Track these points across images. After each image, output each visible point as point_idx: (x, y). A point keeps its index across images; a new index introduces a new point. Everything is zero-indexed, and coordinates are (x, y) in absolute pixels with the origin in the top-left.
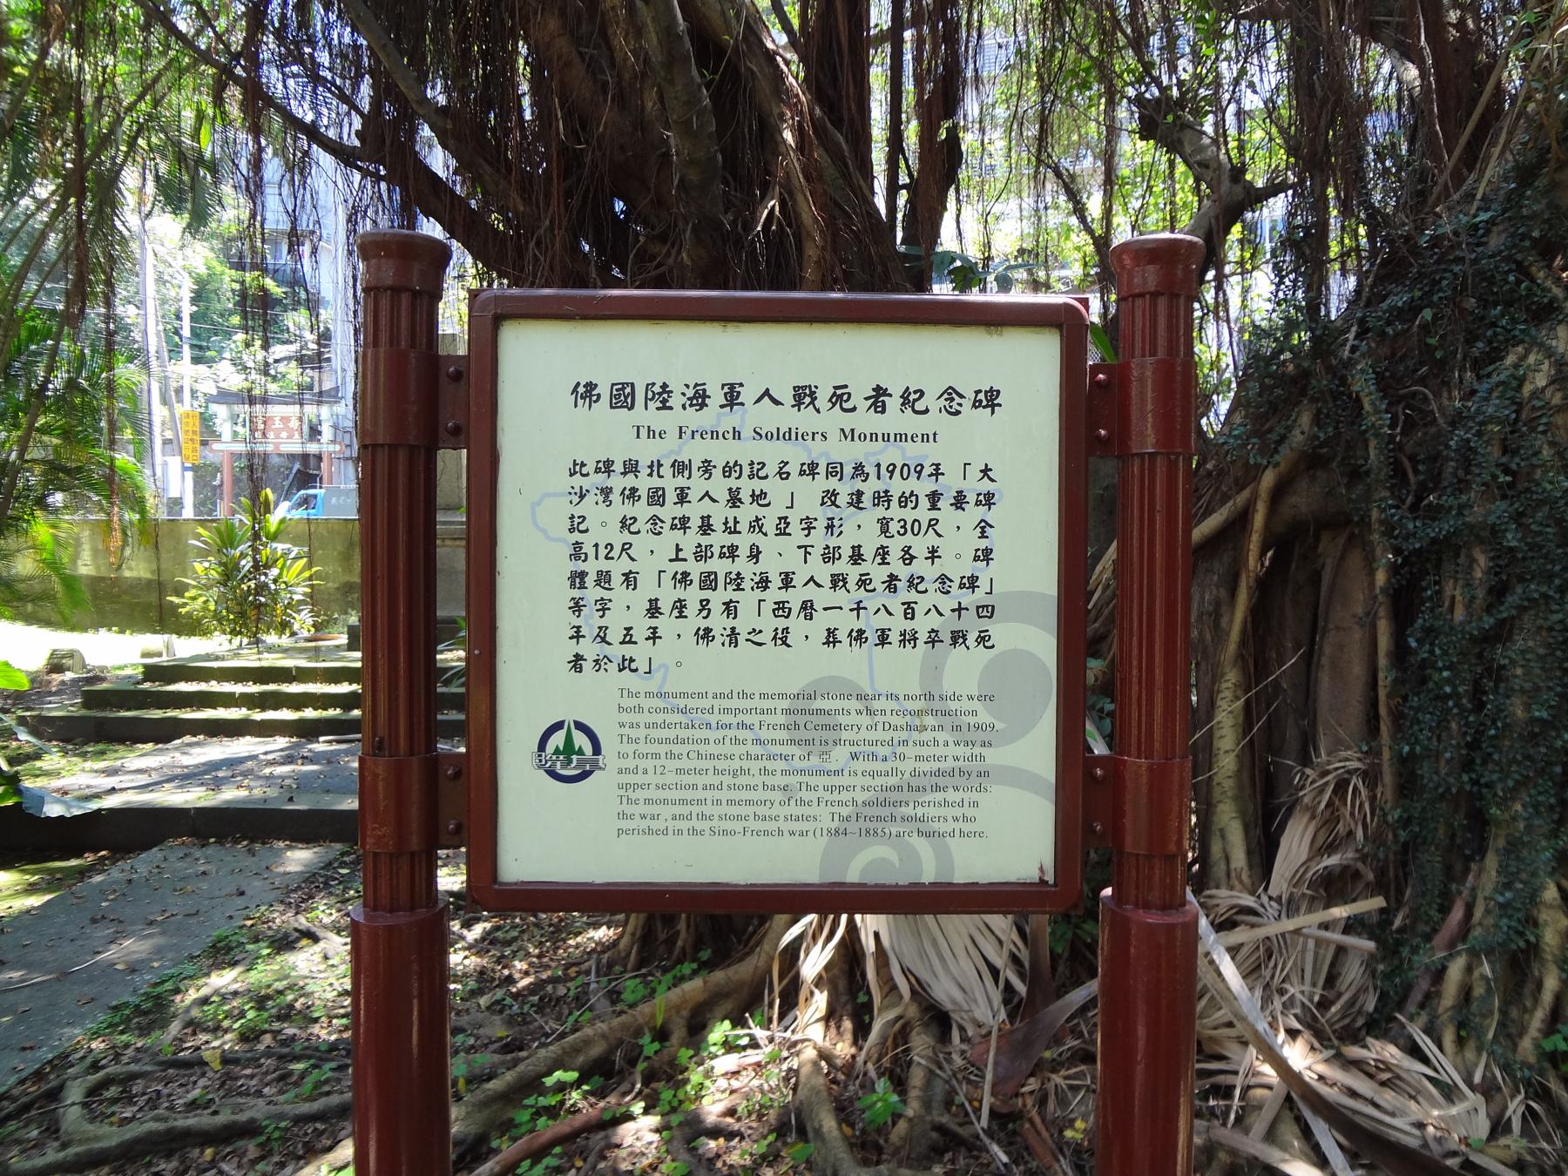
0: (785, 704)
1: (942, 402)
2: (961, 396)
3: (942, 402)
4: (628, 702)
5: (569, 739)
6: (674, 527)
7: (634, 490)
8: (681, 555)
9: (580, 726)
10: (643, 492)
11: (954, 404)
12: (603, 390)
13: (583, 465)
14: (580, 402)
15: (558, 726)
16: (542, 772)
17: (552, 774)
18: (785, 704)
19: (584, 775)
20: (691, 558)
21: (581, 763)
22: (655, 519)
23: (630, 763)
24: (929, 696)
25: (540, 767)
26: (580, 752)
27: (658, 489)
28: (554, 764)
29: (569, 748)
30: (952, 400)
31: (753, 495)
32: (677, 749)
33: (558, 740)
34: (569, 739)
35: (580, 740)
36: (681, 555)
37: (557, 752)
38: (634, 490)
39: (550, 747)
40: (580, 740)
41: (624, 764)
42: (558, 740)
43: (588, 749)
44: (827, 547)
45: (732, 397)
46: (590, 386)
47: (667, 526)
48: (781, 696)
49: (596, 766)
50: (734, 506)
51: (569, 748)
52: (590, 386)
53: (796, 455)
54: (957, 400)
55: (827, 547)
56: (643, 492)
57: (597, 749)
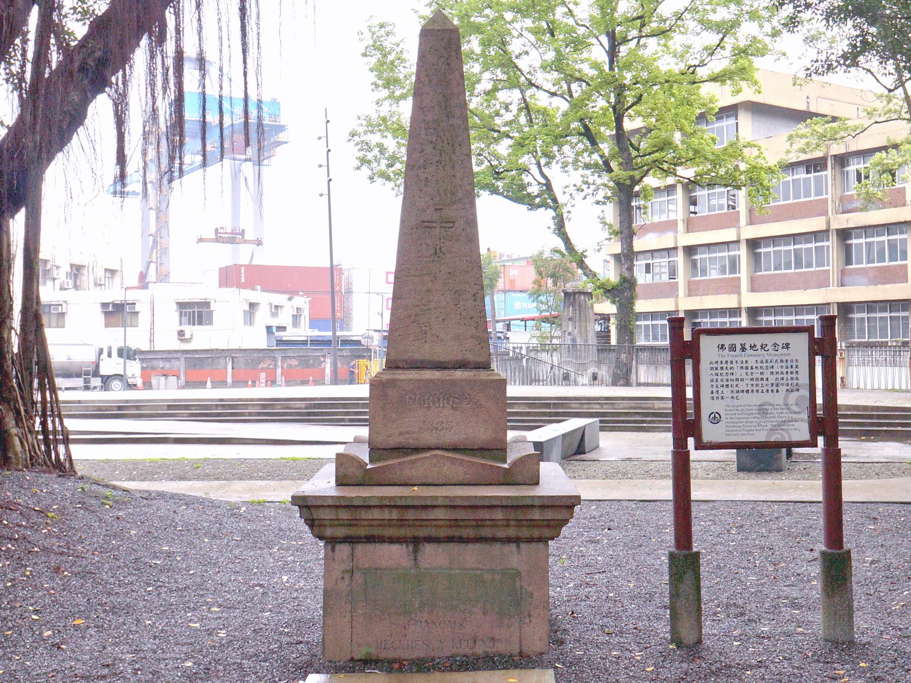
0: (756, 408)
12: (727, 346)
18: (756, 408)
24: (785, 405)
32: (733, 416)
33: (713, 415)
35: (717, 415)
40: (717, 415)
41: (727, 421)
42: (713, 415)
45: (743, 349)
46: (723, 345)
48: (755, 406)
52: (723, 345)
53: (775, 358)
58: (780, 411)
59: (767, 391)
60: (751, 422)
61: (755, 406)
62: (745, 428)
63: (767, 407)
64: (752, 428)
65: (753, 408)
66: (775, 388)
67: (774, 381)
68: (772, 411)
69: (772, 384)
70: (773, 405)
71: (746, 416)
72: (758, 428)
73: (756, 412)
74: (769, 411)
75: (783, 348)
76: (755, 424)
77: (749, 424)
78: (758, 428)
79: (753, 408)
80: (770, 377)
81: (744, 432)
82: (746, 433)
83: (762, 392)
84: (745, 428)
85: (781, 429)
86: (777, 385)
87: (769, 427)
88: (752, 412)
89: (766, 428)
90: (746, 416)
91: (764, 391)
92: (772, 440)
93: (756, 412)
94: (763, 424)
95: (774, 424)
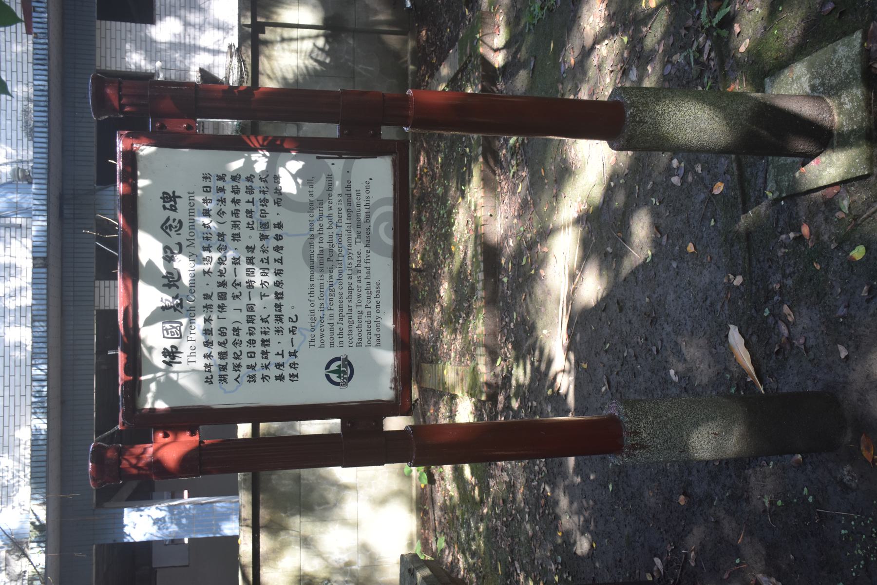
0: (317, 275)
1: (173, 233)
2: (168, 219)
3: (173, 233)
4: (318, 343)
5: (333, 372)
6: (238, 335)
7: (219, 307)
8: (251, 200)
9: (328, 367)
10: (220, 302)
11: (174, 224)
13: (207, 378)
14: (177, 360)
15: (328, 377)
16: (349, 384)
17: (350, 379)
18: (317, 275)
19: (350, 364)
20: (252, 196)
21: (345, 366)
22: (233, 201)
23: (346, 339)
24: (311, 210)
25: (347, 384)
26: (339, 366)
27: (218, 296)
28: (345, 378)
29: (337, 372)
30: (171, 226)
31: (221, 276)
32: (336, 331)
33: (334, 377)
34: (333, 372)
35: (334, 367)
36: (251, 200)
37: (339, 377)
38: (219, 307)
39: (338, 380)
40: (334, 367)
41: (346, 344)
42: (334, 377)
43: (338, 363)
44: (246, 192)
47: (237, 338)
48: (312, 279)
49: (346, 359)
50: (226, 284)
51: (337, 372)
54: (171, 222)
55: (246, 192)
56: (220, 302)
57: (338, 359)
58: (326, 222)
59: (278, 249)
60: (350, 288)
61: (312, 279)
62: (364, 303)
63: (317, 251)
64: (364, 285)
65: (317, 283)
66: (272, 232)
67: (256, 234)
68: (326, 238)
69: (263, 237)
70: (312, 237)
71: (336, 299)
72: (364, 274)
73: (326, 276)
74: (326, 246)
75: (174, 209)
76: (355, 278)
77: (355, 293)
78: (364, 274)
79: (317, 283)
80: (245, 241)
81: (373, 304)
82: (373, 301)
83: (280, 261)
84: (364, 303)
85: (367, 220)
86: (265, 226)
87: (360, 247)
88: (326, 285)
89: (364, 256)
90: (336, 299)
91: (278, 256)
92: (390, 242)
93: (326, 276)
94: (354, 263)
95: (354, 235)
